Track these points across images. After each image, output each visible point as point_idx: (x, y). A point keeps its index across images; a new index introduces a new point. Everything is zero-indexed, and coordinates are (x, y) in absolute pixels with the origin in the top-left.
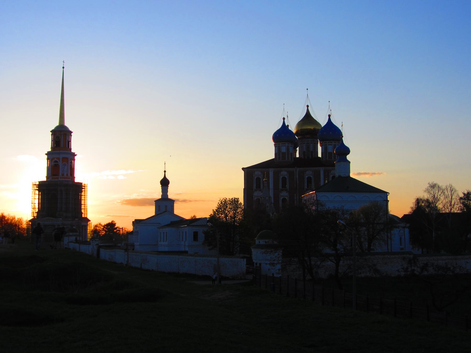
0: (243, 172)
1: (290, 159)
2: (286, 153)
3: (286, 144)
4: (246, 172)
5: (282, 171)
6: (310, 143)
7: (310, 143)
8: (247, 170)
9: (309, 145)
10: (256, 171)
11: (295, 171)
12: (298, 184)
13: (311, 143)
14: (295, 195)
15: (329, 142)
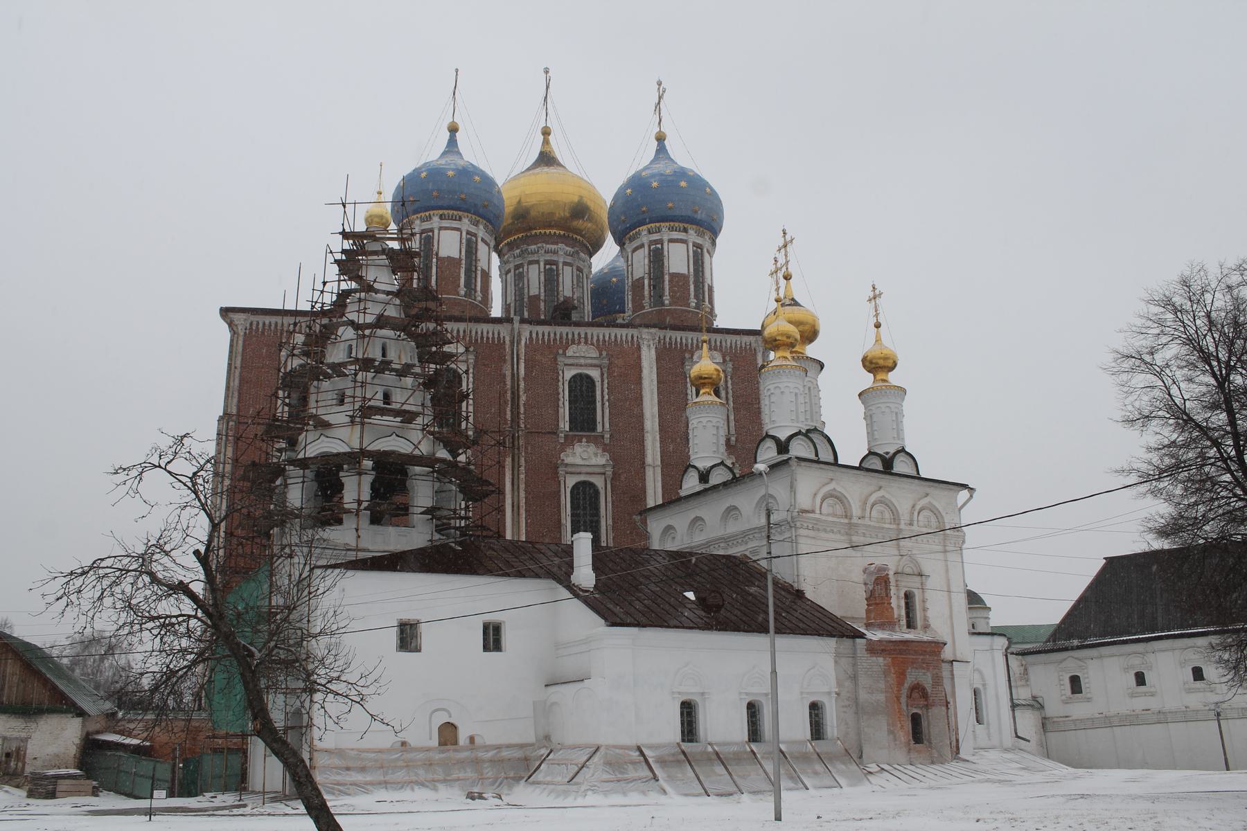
6: (561, 260)
7: (561, 260)
8: (251, 324)
11: (507, 339)
12: (522, 410)
13: (565, 264)
14: (508, 461)
15: (671, 229)
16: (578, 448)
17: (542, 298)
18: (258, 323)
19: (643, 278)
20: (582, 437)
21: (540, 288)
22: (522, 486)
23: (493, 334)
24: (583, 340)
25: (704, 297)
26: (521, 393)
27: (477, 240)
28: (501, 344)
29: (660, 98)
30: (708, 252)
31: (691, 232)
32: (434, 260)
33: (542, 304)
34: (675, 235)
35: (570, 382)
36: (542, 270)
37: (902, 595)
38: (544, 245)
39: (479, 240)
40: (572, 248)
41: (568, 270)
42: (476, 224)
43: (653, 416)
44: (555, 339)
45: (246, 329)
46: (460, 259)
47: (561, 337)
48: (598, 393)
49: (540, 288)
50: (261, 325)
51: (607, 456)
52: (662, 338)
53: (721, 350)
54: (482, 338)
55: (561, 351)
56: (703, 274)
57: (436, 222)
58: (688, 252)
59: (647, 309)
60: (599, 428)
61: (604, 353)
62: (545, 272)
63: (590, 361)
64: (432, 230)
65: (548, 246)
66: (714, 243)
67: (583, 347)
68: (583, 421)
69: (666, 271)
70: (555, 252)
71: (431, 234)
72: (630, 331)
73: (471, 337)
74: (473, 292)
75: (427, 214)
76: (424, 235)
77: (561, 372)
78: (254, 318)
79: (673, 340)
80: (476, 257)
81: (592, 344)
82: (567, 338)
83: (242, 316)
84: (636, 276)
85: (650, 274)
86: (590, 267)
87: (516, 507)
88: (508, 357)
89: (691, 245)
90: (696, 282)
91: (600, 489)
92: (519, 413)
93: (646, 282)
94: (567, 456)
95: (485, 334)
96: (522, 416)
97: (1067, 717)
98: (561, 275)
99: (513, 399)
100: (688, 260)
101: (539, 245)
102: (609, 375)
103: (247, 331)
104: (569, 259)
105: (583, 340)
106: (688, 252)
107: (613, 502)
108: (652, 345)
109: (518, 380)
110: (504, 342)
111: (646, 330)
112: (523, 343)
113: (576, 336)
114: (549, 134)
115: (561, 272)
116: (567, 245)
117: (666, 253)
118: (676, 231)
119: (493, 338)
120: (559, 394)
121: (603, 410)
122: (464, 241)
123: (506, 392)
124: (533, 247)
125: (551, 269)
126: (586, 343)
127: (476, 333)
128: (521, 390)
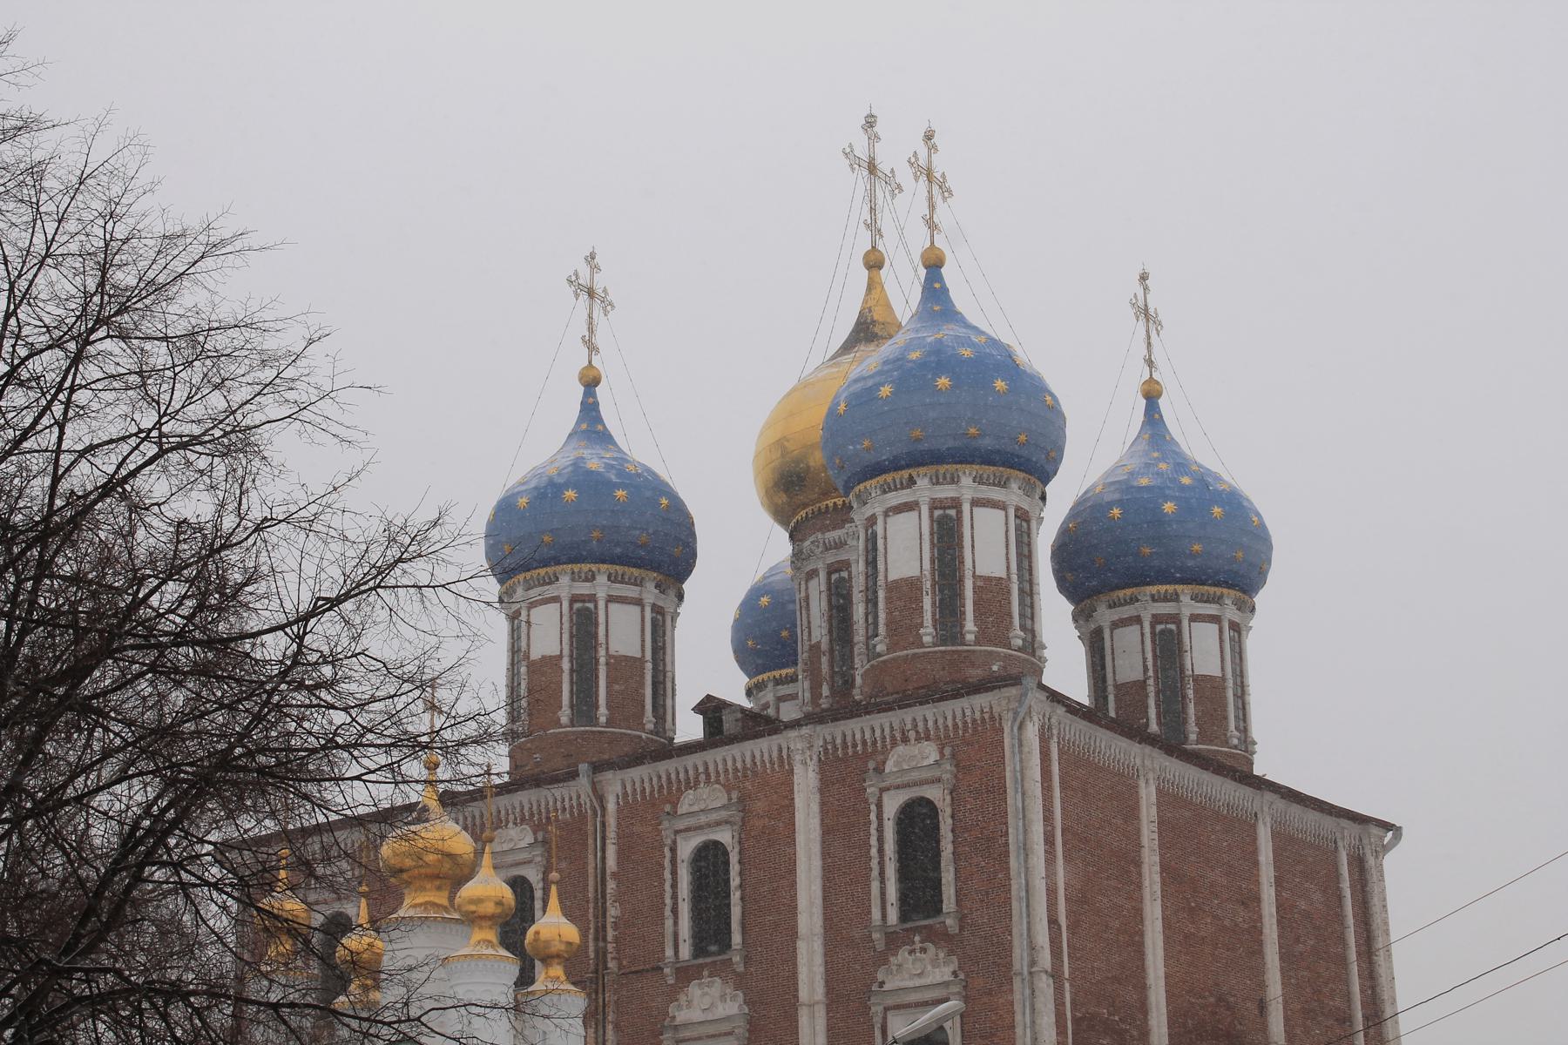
16: (694, 990)
24: (702, 777)
34: (895, 498)
46: (561, 657)
63: (714, 817)
67: (703, 791)
81: (718, 782)
94: (679, 1008)
105: (702, 777)
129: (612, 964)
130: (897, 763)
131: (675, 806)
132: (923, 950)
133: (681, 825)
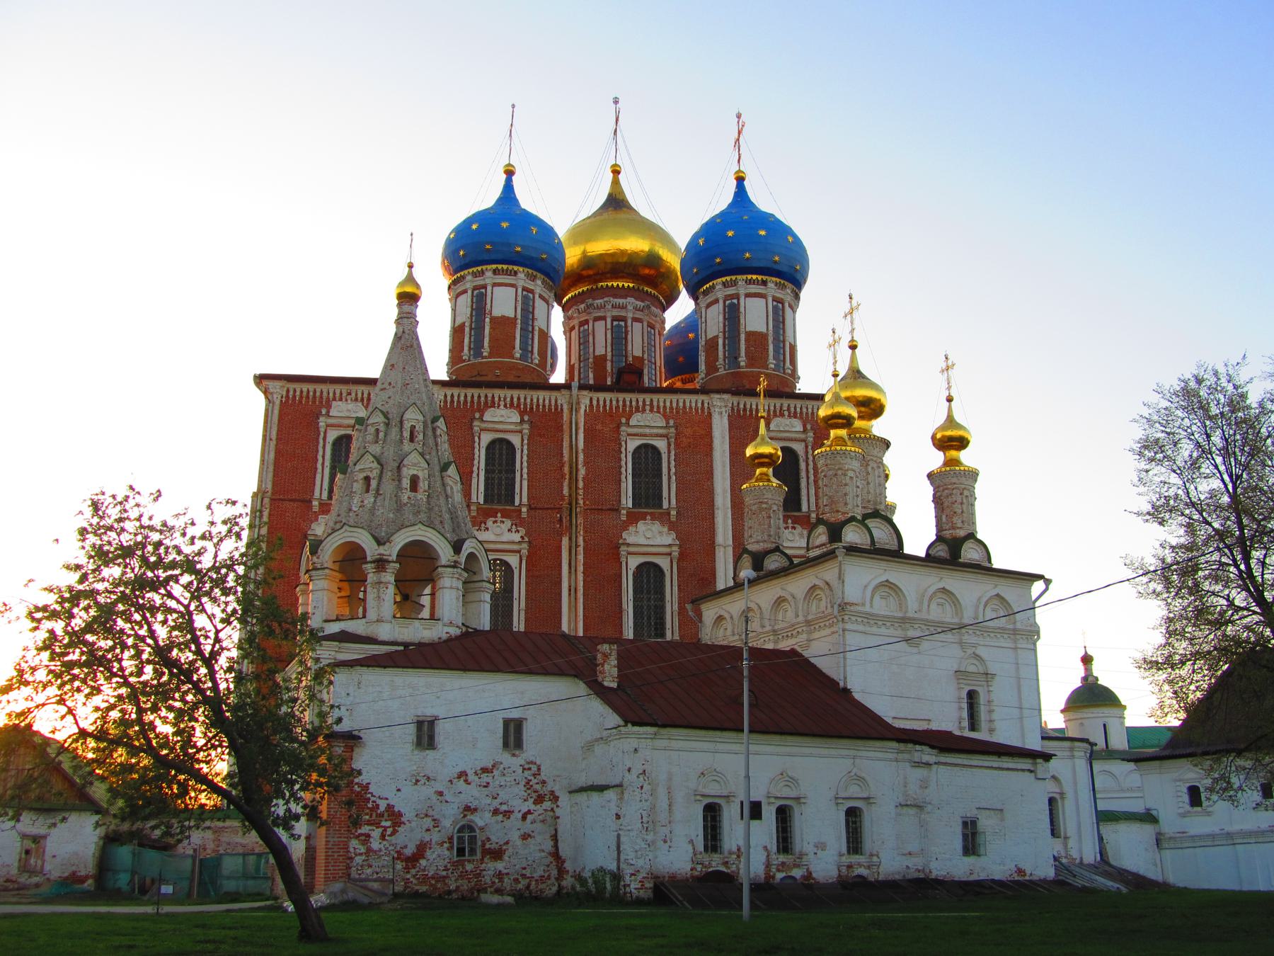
0: (258, 401)
1: (536, 355)
2: (519, 321)
3: (521, 276)
4: (278, 402)
5: (493, 406)
6: (630, 315)
7: (630, 315)
8: (288, 391)
9: (626, 326)
10: (341, 399)
11: (565, 407)
12: (581, 484)
13: (635, 320)
14: (565, 541)
15: (750, 282)
16: (641, 526)
17: (609, 357)
18: (295, 391)
19: (717, 337)
20: (646, 514)
21: (606, 347)
22: (581, 568)
23: (550, 401)
24: (648, 408)
25: (784, 358)
26: (580, 466)
27: (534, 297)
28: (558, 413)
29: (739, 133)
30: (790, 306)
31: (771, 285)
32: (487, 320)
33: (609, 364)
34: (754, 289)
35: (634, 453)
36: (609, 326)
37: (964, 695)
38: (612, 299)
39: (537, 296)
40: (643, 301)
41: (637, 326)
42: (533, 278)
43: (724, 491)
44: (618, 407)
45: (282, 397)
47: (624, 405)
48: (665, 465)
49: (606, 347)
50: (298, 393)
51: (673, 535)
52: (735, 404)
53: (801, 418)
54: (538, 405)
55: (624, 420)
56: (784, 332)
57: (489, 278)
58: (767, 308)
59: (722, 372)
60: (665, 505)
61: (671, 422)
62: (612, 329)
63: (655, 431)
64: (485, 287)
65: (616, 300)
66: (797, 297)
68: (648, 497)
69: (742, 329)
70: (623, 307)
71: (483, 290)
72: (701, 398)
73: (525, 404)
74: (530, 355)
75: (479, 268)
76: (476, 292)
77: (623, 443)
78: (292, 386)
79: (748, 407)
80: (533, 316)
81: (658, 412)
82: (631, 406)
83: (278, 384)
84: (710, 336)
85: (724, 332)
86: (663, 322)
87: (573, 590)
88: (566, 427)
89: (770, 299)
90: (776, 339)
91: (666, 571)
92: (577, 488)
93: (721, 341)
95: (541, 401)
96: (581, 492)
97: (1183, 833)
98: (630, 333)
99: (571, 473)
100: (767, 316)
101: (605, 299)
102: (677, 445)
103: (284, 399)
104: (639, 315)
105: (648, 408)
106: (767, 308)
107: (679, 586)
108: (724, 413)
109: (577, 452)
110: (562, 410)
111: (718, 396)
112: (582, 411)
113: (641, 403)
114: (619, 173)
115: (630, 329)
116: (636, 299)
117: (742, 309)
118: (754, 284)
119: (550, 405)
120: (621, 467)
121: (669, 485)
122: (519, 298)
123: (563, 466)
124: (599, 302)
125: (619, 326)
126: (651, 410)
127: (532, 400)
128: (580, 463)
129: (581, 502)
130: (777, 426)
131: (628, 420)
132: (794, 528)
133: (630, 430)
